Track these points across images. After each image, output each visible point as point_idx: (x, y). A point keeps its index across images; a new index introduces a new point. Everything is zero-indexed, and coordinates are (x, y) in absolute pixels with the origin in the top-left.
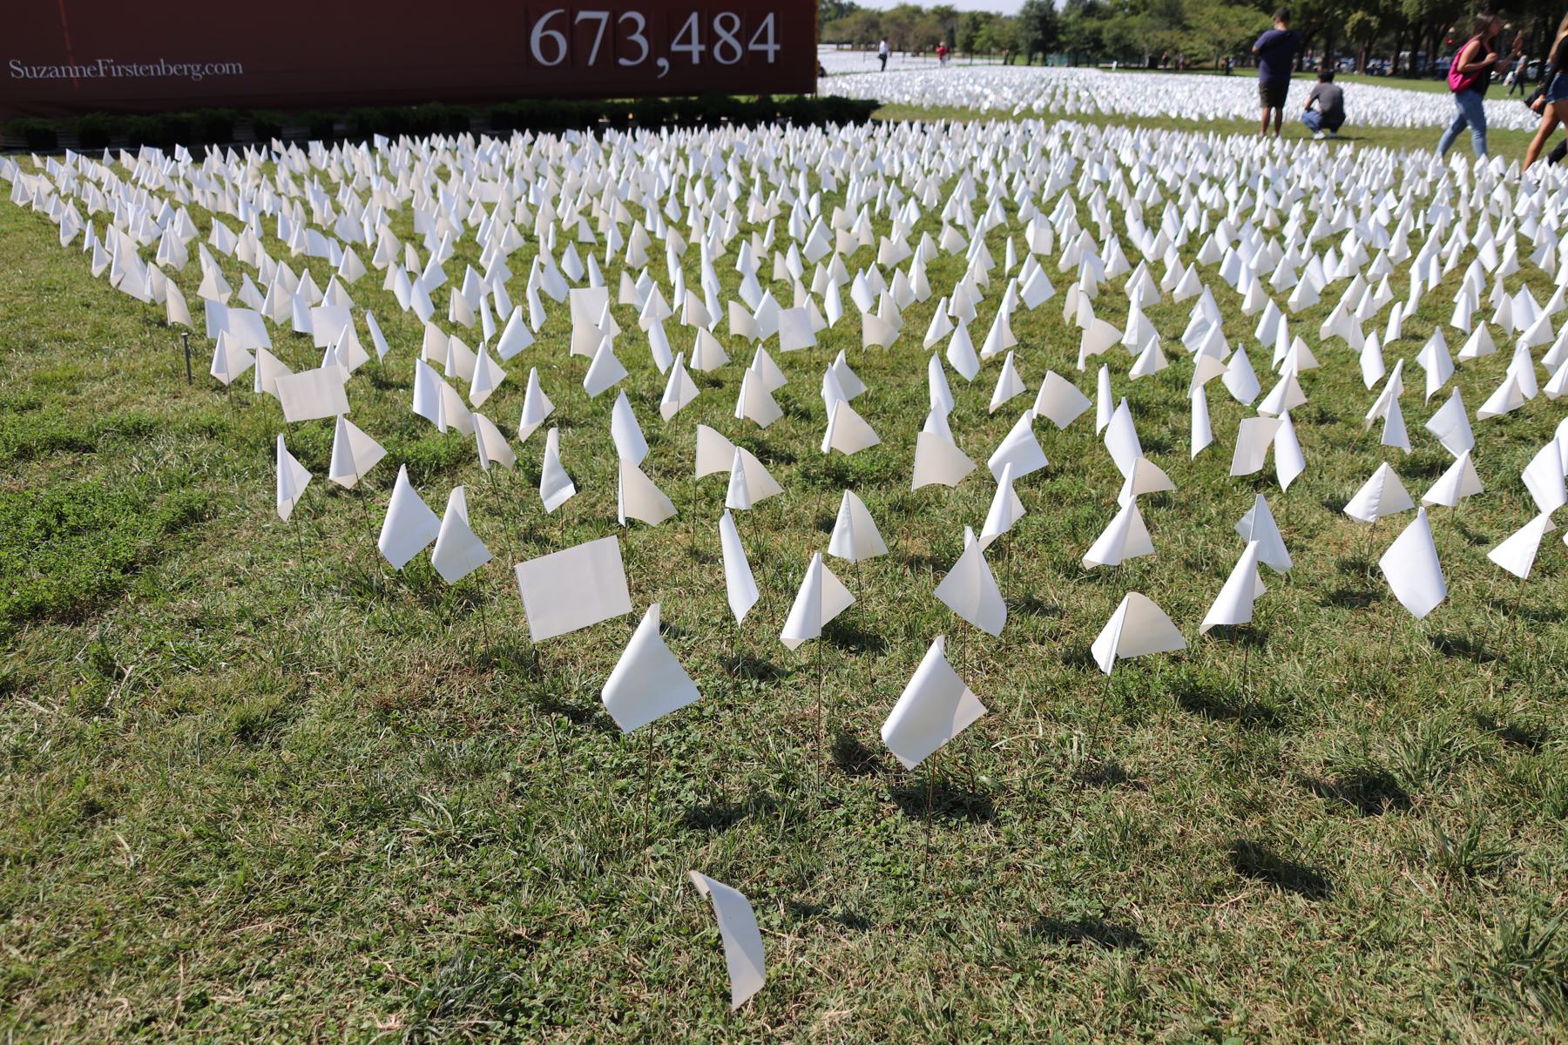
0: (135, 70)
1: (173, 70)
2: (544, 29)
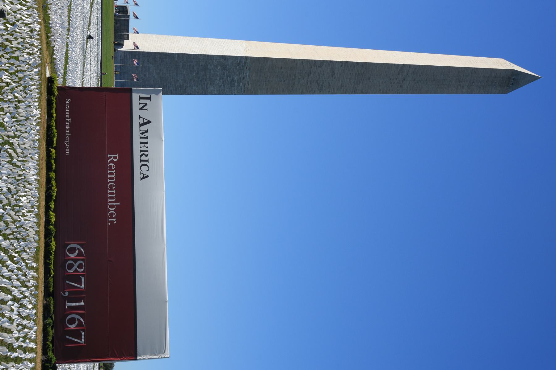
0: (68, 127)
1: (67, 137)
2: (79, 249)
